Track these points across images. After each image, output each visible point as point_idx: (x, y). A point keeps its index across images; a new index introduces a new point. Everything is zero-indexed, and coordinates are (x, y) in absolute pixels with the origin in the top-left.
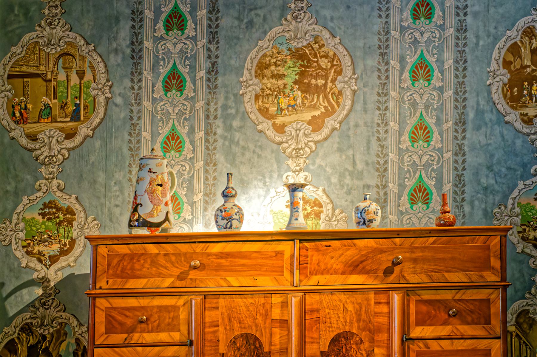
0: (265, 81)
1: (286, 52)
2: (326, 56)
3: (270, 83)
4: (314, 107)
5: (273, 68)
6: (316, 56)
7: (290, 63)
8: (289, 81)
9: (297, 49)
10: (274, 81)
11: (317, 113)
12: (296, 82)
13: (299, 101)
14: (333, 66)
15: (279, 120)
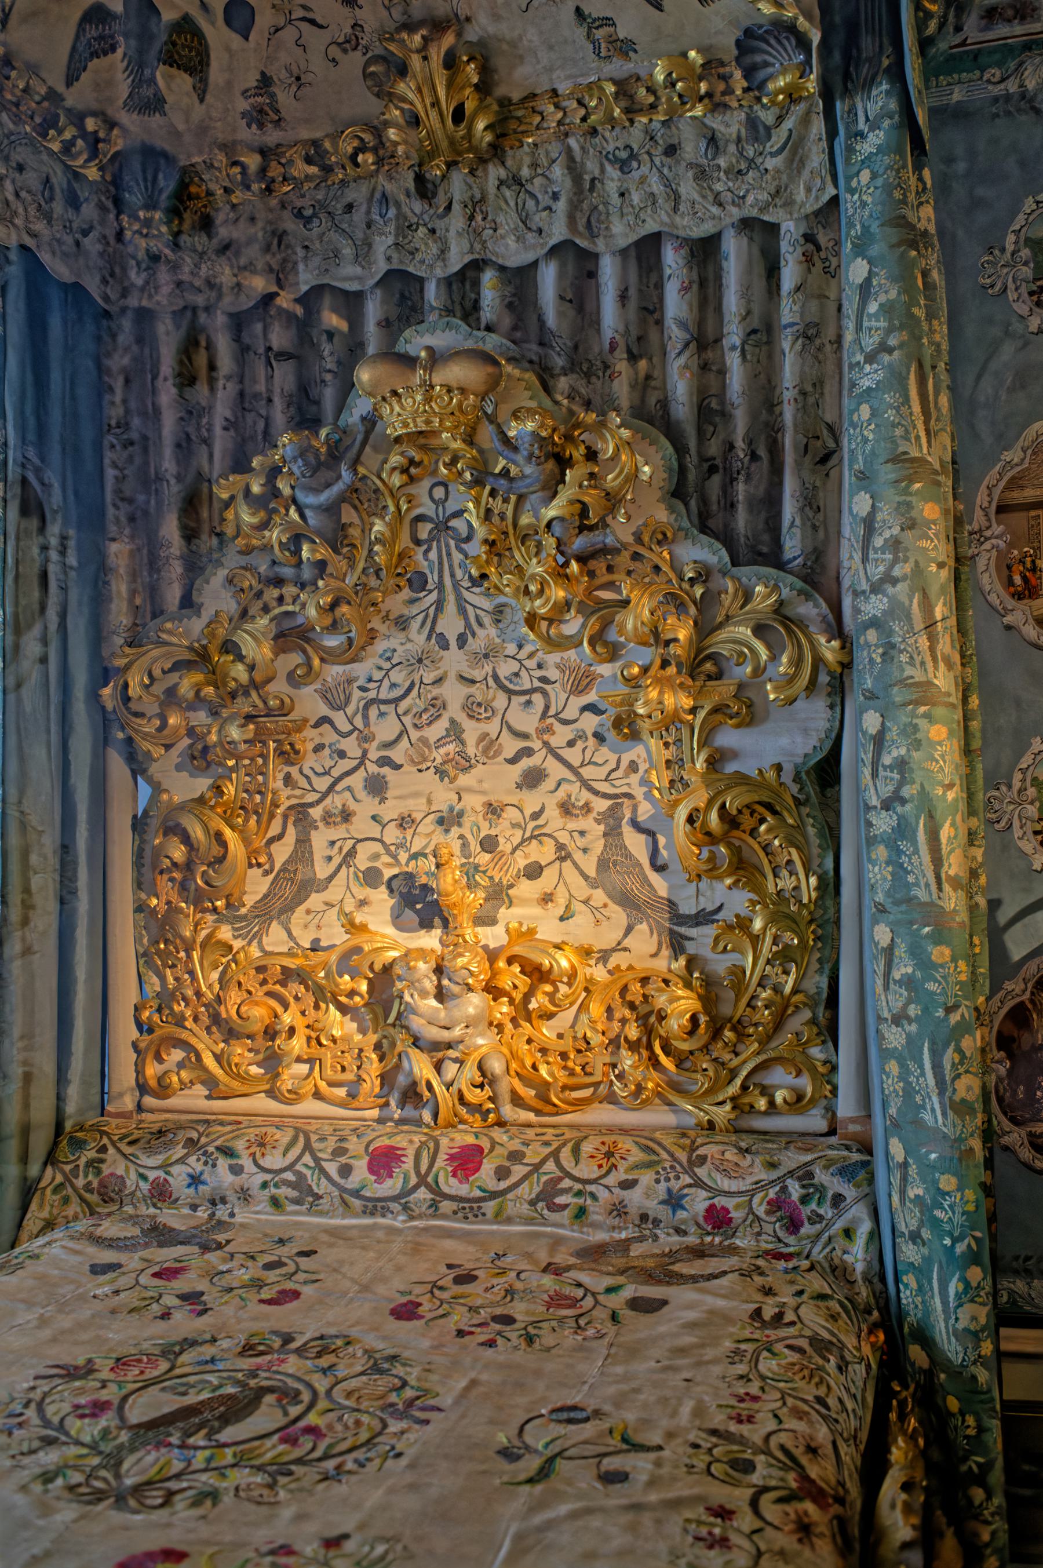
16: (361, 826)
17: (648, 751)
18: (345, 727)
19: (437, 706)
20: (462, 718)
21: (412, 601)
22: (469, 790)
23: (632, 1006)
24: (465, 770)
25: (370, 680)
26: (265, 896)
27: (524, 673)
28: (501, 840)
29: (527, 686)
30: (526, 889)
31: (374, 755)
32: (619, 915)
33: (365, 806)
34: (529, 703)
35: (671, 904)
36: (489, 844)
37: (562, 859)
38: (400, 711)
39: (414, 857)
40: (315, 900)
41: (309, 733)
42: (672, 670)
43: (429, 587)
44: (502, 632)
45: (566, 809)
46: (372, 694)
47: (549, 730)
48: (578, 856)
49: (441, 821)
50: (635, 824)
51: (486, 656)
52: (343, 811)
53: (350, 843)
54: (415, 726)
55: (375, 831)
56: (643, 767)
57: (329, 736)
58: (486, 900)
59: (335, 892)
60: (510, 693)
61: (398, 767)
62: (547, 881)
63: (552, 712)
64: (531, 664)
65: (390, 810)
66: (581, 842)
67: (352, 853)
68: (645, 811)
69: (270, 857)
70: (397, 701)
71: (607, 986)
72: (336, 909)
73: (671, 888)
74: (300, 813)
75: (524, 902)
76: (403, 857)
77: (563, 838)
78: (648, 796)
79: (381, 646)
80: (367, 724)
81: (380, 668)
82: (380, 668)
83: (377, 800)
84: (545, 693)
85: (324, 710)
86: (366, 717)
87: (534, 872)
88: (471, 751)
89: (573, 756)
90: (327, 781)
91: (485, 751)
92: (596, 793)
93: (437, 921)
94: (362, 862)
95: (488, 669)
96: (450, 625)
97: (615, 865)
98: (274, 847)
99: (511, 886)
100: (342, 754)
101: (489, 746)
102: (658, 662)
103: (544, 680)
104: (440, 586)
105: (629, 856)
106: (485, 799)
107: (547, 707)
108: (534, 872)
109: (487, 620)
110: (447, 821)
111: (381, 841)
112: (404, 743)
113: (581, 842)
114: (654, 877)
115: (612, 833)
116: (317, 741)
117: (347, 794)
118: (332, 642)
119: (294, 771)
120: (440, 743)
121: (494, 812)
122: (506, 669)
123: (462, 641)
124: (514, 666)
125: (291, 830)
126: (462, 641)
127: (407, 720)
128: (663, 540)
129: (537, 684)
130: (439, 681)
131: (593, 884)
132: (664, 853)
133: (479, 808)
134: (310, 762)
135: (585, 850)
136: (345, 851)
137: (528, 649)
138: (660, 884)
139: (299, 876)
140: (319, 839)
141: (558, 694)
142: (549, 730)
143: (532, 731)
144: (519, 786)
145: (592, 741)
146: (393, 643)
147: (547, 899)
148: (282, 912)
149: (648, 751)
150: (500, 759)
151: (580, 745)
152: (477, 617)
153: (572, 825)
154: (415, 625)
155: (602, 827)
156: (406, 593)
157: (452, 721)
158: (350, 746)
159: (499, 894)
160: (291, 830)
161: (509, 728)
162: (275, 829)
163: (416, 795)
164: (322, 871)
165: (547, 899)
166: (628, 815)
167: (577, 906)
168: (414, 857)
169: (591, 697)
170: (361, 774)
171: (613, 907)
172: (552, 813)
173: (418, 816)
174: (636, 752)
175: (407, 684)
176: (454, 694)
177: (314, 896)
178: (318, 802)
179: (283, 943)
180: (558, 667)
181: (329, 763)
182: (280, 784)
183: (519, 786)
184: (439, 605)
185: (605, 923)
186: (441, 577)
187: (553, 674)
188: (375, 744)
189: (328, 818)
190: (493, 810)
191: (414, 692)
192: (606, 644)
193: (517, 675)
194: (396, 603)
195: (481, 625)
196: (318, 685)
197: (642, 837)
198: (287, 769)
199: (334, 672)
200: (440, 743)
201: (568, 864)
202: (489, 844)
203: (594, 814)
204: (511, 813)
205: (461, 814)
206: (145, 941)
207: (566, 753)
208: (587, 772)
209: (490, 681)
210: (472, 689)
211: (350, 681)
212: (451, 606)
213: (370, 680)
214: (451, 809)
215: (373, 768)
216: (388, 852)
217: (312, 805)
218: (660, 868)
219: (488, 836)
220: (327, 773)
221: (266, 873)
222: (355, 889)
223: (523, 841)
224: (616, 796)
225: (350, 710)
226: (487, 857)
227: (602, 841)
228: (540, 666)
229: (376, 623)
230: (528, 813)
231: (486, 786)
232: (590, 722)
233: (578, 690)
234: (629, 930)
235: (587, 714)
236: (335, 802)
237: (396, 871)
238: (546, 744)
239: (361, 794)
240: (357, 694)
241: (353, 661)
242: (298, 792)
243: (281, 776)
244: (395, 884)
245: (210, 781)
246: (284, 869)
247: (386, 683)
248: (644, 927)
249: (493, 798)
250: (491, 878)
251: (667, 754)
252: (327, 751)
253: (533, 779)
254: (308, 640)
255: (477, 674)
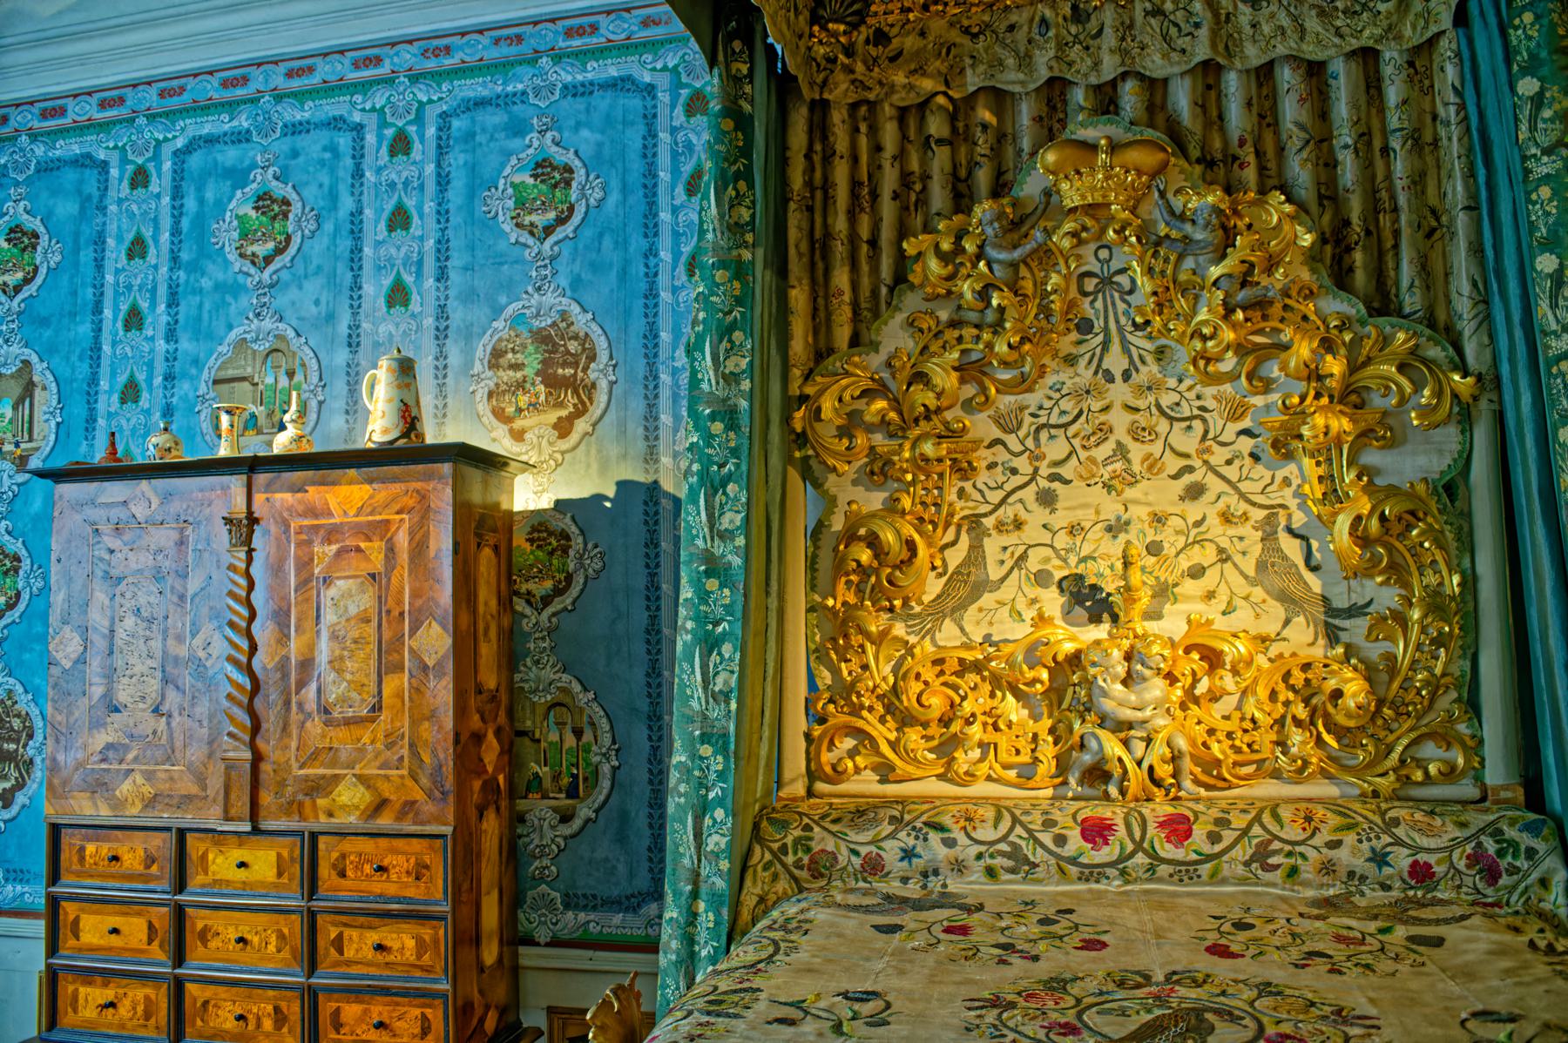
0: (501, 373)
1: (526, 334)
2: (576, 337)
3: (508, 376)
4: (560, 405)
5: (510, 355)
6: (563, 338)
7: (531, 349)
8: (529, 372)
9: (540, 330)
10: (511, 373)
11: (564, 413)
12: (537, 374)
13: (542, 398)
14: (584, 350)
15: (518, 424)
16: (1032, 533)
17: (1300, 469)
18: (1017, 448)
19: (1104, 431)
20: (1127, 441)
21: (1080, 343)
22: (1136, 502)
23: (1292, 688)
24: (1131, 484)
25: (1041, 408)
26: (939, 597)
27: (1184, 403)
28: (1166, 545)
29: (1187, 414)
30: (1189, 587)
31: (1044, 471)
32: (1277, 610)
33: (1036, 516)
34: (1189, 427)
35: (1325, 599)
36: (1154, 549)
37: (1224, 561)
38: (1070, 434)
39: (1084, 560)
40: (987, 599)
41: (983, 452)
42: (1325, 400)
43: (1096, 330)
44: (1163, 370)
45: (1227, 518)
46: (1043, 420)
47: (1208, 450)
48: (1237, 558)
49: (1109, 529)
50: (1290, 530)
51: (1149, 388)
52: (1015, 520)
53: (1021, 549)
54: (1084, 447)
55: (1046, 537)
56: (1296, 482)
57: (1001, 455)
58: (1153, 597)
59: (1006, 591)
60: (1172, 419)
61: (1067, 482)
62: (1210, 580)
63: (1211, 435)
64: (1191, 395)
65: (1060, 519)
66: (1240, 546)
67: (1023, 557)
68: (1299, 520)
69: (944, 560)
70: (1065, 426)
71: (1269, 671)
72: (1008, 608)
73: (1324, 586)
74: (974, 521)
75: (1188, 598)
76: (1073, 560)
77: (1224, 543)
78: (1302, 506)
79: (1050, 379)
80: (1038, 445)
81: (1050, 398)
82: (1050, 398)
83: (1048, 511)
84: (1204, 420)
85: (998, 434)
86: (1037, 439)
87: (1197, 572)
88: (1136, 468)
89: (1232, 473)
90: (1000, 494)
91: (1150, 468)
92: (1254, 504)
93: (1105, 616)
94: (1033, 564)
95: (1151, 399)
96: (1115, 361)
97: (1273, 565)
98: (947, 552)
99: (1176, 585)
100: (1014, 471)
101: (1153, 465)
102: (1312, 393)
103: (1202, 408)
104: (1106, 330)
105: (1285, 558)
106: (1150, 509)
107: (1206, 432)
108: (1197, 572)
109: (1149, 358)
110: (1114, 529)
111: (1052, 546)
112: (1074, 461)
113: (1240, 546)
114: (1309, 577)
115: (1269, 537)
116: (991, 459)
117: (1019, 506)
118: (1005, 375)
119: (968, 485)
120: (1107, 461)
121: (1159, 521)
122: (1167, 400)
123: (1126, 376)
124: (1175, 397)
125: (964, 538)
126: (1126, 376)
127: (1076, 442)
128: (1311, 295)
129: (1196, 412)
130: (1106, 409)
131: (1252, 582)
132: (1317, 555)
133: (1145, 518)
134: (983, 478)
135: (1244, 553)
136: (1017, 555)
137: (1187, 382)
138: (1315, 582)
139: (972, 578)
140: (992, 545)
141: (1216, 421)
142: (1208, 450)
143: (1192, 452)
144: (1182, 499)
145: (1248, 461)
146: (1063, 377)
147: (1210, 595)
148: (953, 611)
149: (1300, 469)
150: (1164, 475)
151: (1237, 463)
152: (1141, 357)
153: (1232, 531)
154: (1083, 362)
155: (1260, 533)
156: (1074, 336)
157: (1119, 444)
158: (1023, 464)
159: (1163, 592)
160: (964, 538)
161: (1172, 449)
162: (950, 535)
163: (1085, 506)
164: (994, 573)
165: (1210, 595)
166: (1283, 522)
167: (1238, 602)
168: (1084, 560)
169: (1246, 423)
170: (1032, 488)
171: (1271, 602)
172: (1213, 521)
173: (1087, 525)
174: (1290, 469)
175: (1076, 412)
176: (1120, 420)
177: (986, 595)
178: (991, 513)
179: (955, 638)
180: (1215, 398)
181: (1001, 479)
182: (953, 497)
183: (1182, 499)
184: (1105, 345)
185: (1264, 617)
186: (1106, 322)
187: (1210, 403)
188: (1045, 462)
189: (1000, 527)
190: (1159, 519)
191: (1083, 418)
192: (1261, 379)
193: (1178, 404)
194: (1066, 343)
195: (1143, 362)
196: (991, 412)
197: (1298, 541)
198: (961, 484)
199: (1007, 401)
200: (1107, 461)
201: (1228, 565)
202: (1154, 549)
203: (1252, 522)
204: (1175, 522)
205: (1127, 523)
206: (818, 638)
207: (1225, 471)
208: (1244, 486)
209: (1154, 410)
210: (1137, 416)
211: (1022, 409)
212: (1116, 347)
213: (1041, 408)
214: (1118, 519)
215: (1044, 483)
216: (1059, 557)
217: (985, 515)
218: (1314, 569)
219: (1153, 542)
220: (1000, 487)
221: (940, 575)
222: (1026, 589)
223: (1186, 546)
224: (1272, 507)
225: (1021, 433)
226: (1153, 560)
227: (1260, 546)
228: (1199, 397)
229: (1046, 360)
230: (1191, 521)
231: (1151, 498)
232: (1246, 444)
233: (1234, 416)
234: (1287, 622)
235: (1242, 437)
236: (1007, 513)
237: (1066, 573)
238: (1206, 462)
239: (1033, 506)
240: (1028, 420)
241: (1026, 391)
242: (971, 504)
243: (954, 490)
244: (1065, 585)
245: (886, 494)
246: (957, 572)
247: (1056, 411)
248: (1301, 619)
249: (1157, 509)
250: (1157, 578)
251: (1321, 471)
252: (1000, 469)
253: (1195, 492)
254: (985, 374)
255: (1141, 404)
